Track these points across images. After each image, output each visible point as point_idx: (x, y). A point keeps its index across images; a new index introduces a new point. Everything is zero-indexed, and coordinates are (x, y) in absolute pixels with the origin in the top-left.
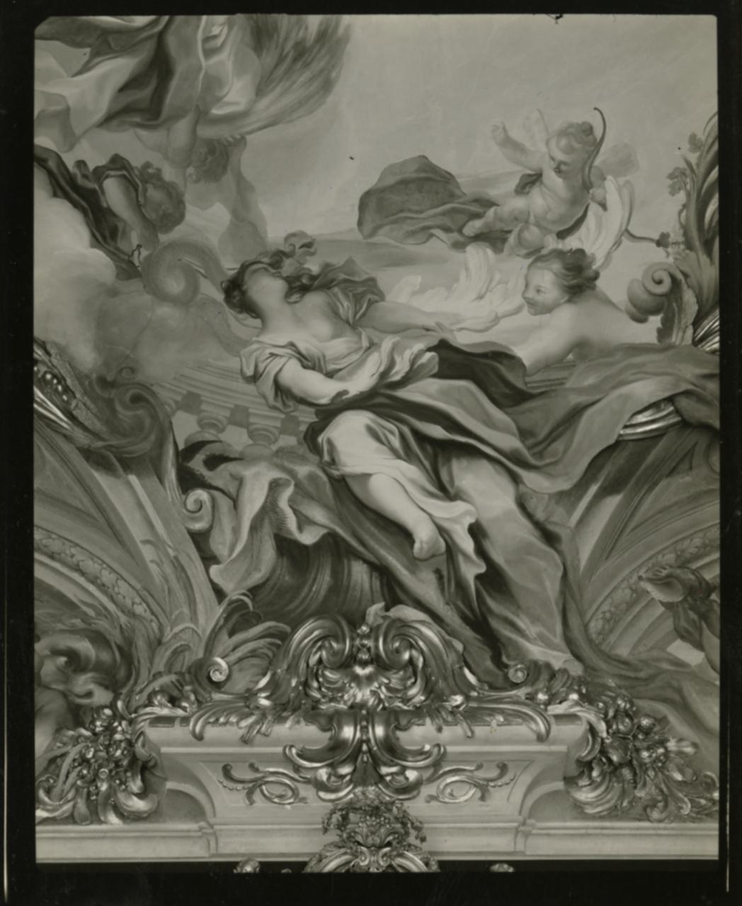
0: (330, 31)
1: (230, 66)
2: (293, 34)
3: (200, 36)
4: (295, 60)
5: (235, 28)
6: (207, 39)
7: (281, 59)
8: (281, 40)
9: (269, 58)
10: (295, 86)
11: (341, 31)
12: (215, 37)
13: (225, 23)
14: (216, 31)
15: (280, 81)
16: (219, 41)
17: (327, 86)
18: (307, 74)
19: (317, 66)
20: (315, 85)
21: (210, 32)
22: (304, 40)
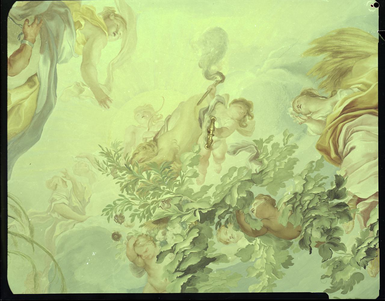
0: (318, 50)
1: (366, 75)
2: (331, 62)
3: (364, 94)
4: (341, 53)
5: (348, 84)
6: (363, 90)
7: (346, 58)
8: (338, 64)
9: (349, 63)
10: (352, 44)
11: (314, 45)
12: (359, 88)
13: (350, 89)
14: (356, 90)
15: (356, 51)
16: (360, 86)
17: (341, 32)
18: (343, 43)
19: (337, 43)
20: (345, 37)
21: (358, 91)
22: (330, 56)
